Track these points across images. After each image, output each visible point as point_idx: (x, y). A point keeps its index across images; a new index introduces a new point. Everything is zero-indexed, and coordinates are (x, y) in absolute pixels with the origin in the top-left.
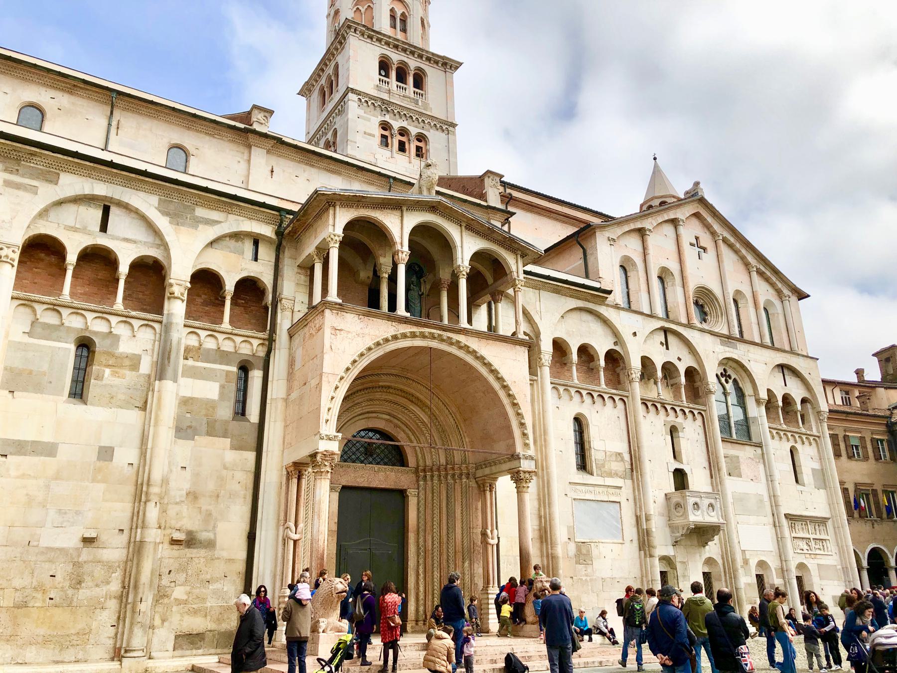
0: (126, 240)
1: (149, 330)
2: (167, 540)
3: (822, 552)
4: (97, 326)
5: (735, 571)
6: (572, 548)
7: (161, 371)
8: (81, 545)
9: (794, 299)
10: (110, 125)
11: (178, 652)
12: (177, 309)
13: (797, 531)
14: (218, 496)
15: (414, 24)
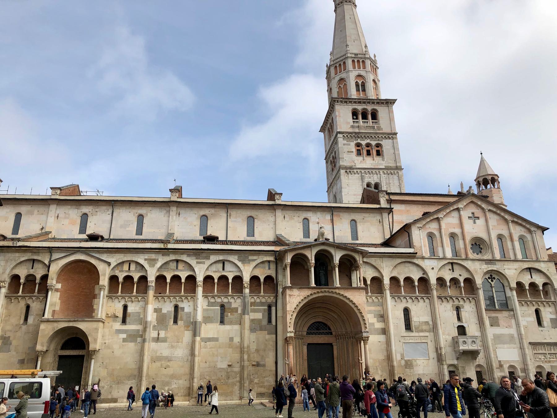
0: (230, 271)
1: (240, 299)
2: (251, 365)
3: (555, 360)
4: (226, 300)
5: (492, 370)
6: (403, 363)
7: (244, 312)
8: (228, 367)
9: (539, 232)
10: (227, 216)
11: (258, 398)
12: (247, 291)
13: (537, 350)
14: (265, 350)
15: (370, 85)
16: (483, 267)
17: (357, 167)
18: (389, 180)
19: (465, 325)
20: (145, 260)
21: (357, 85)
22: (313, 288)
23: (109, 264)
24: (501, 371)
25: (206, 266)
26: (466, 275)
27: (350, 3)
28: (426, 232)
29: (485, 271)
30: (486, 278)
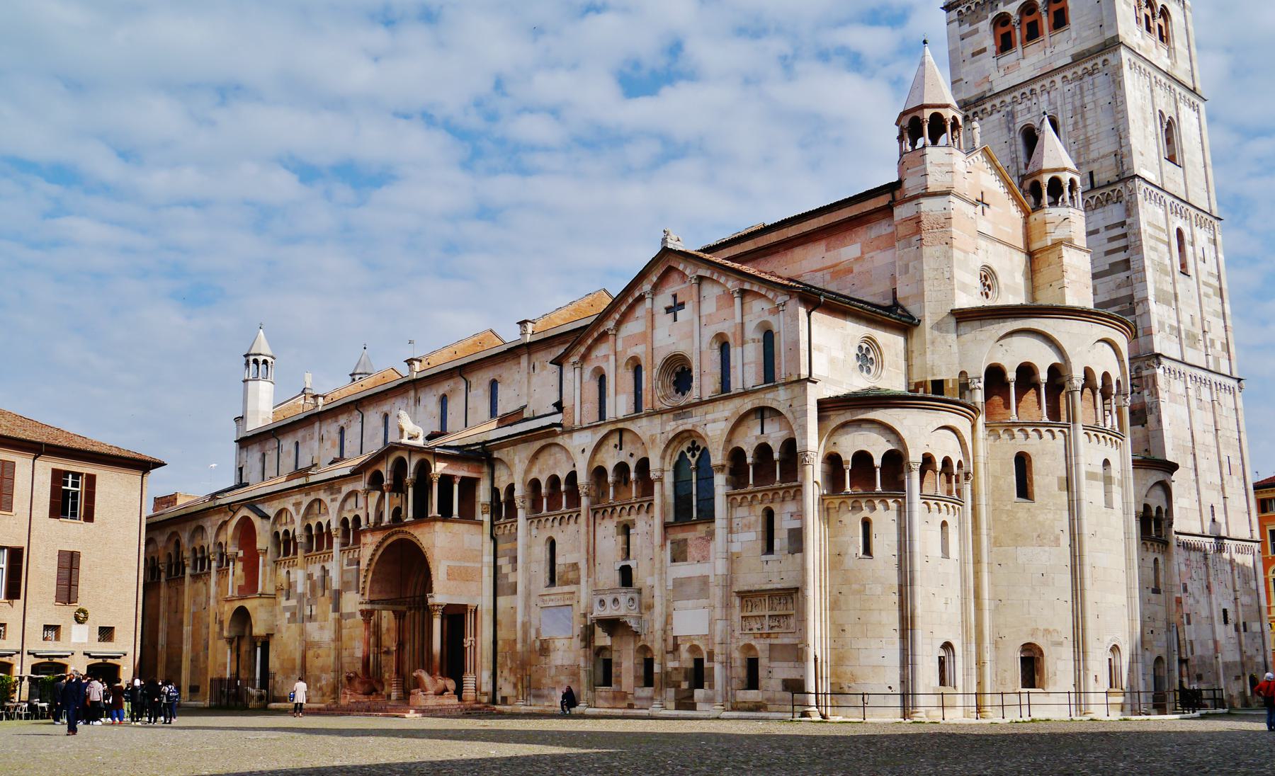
6: (538, 644)
13: (749, 608)
16: (668, 428)
18: (1082, 97)
19: (632, 563)
20: (294, 505)
22: (385, 528)
23: (265, 517)
25: (337, 504)
26: (640, 455)
28: (591, 368)
29: (671, 435)
30: (683, 453)
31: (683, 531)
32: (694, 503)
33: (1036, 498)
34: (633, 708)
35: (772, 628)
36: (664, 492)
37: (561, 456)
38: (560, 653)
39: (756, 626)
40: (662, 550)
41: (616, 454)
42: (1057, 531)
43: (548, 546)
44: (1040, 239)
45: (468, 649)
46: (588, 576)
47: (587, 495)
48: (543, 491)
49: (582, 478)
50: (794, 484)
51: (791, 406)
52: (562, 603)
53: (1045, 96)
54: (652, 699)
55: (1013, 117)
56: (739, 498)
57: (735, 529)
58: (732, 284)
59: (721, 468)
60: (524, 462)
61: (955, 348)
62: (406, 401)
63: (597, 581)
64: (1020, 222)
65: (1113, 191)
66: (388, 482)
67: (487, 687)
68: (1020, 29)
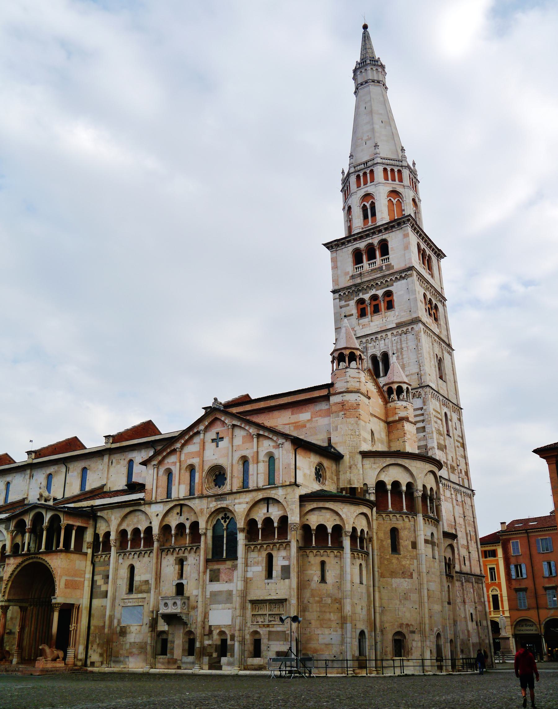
6: (118, 629)
16: (211, 506)
17: (358, 336)
18: (401, 344)
19: (184, 582)
21: (364, 209)
24: (209, 640)
26: (193, 519)
27: (367, 84)
28: (164, 469)
29: (213, 510)
30: (219, 519)
31: (218, 564)
32: (225, 548)
33: (402, 552)
34: (181, 669)
35: (271, 621)
36: (206, 542)
37: (142, 517)
38: (134, 635)
39: (261, 620)
40: (204, 575)
41: (177, 518)
42: (411, 571)
43: (129, 570)
44: (393, 416)
45: (72, 632)
46: (156, 588)
47: (158, 540)
48: (129, 537)
49: (156, 531)
50: (286, 541)
51: (285, 498)
52: (137, 604)
53: (383, 341)
54: (193, 663)
55: (367, 350)
56: (252, 547)
57: (249, 564)
58: (253, 431)
59: (242, 530)
60: (118, 519)
61: (361, 472)
62: (23, 476)
63: (161, 591)
64: (383, 407)
65: (417, 392)
66: (29, 527)
67: (81, 656)
68: (370, 307)
